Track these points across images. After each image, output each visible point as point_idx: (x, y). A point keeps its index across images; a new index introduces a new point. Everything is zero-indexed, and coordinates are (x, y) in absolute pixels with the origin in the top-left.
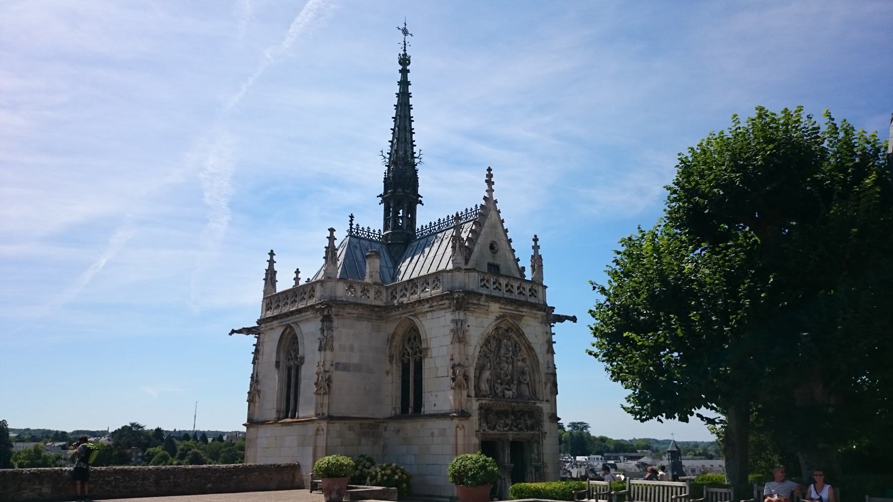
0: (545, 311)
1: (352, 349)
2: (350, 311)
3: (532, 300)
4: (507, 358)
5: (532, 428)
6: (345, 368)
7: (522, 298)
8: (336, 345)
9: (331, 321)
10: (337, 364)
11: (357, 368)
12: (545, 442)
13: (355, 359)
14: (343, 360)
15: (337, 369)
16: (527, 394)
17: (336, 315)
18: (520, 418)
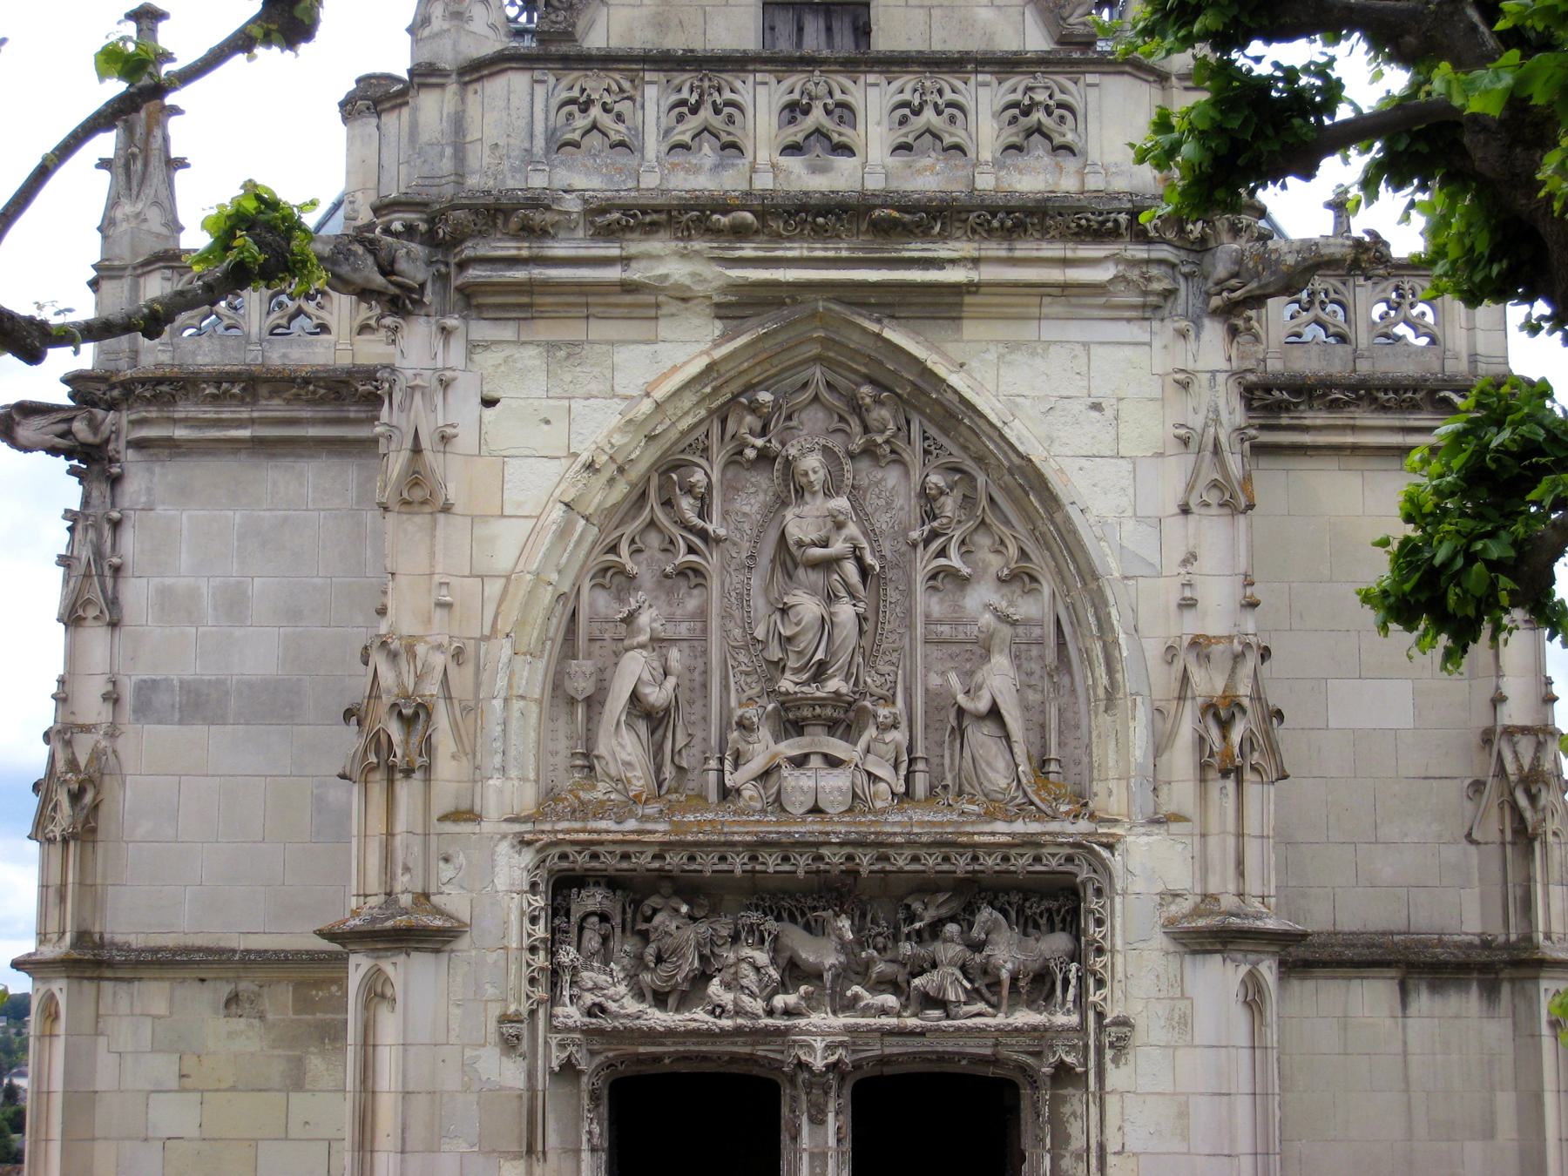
0: (1141, 236)
1: (234, 605)
2: (209, 412)
3: (1033, 179)
4: (829, 565)
5: (1039, 985)
6: (198, 704)
7: (928, 179)
8: (136, 593)
9: (115, 481)
10: (147, 688)
11: (272, 703)
12: (1116, 1077)
13: (257, 655)
14: (188, 666)
15: (144, 709)
16: (998, 777)
17: (140, 445)
18: (934, 930)
